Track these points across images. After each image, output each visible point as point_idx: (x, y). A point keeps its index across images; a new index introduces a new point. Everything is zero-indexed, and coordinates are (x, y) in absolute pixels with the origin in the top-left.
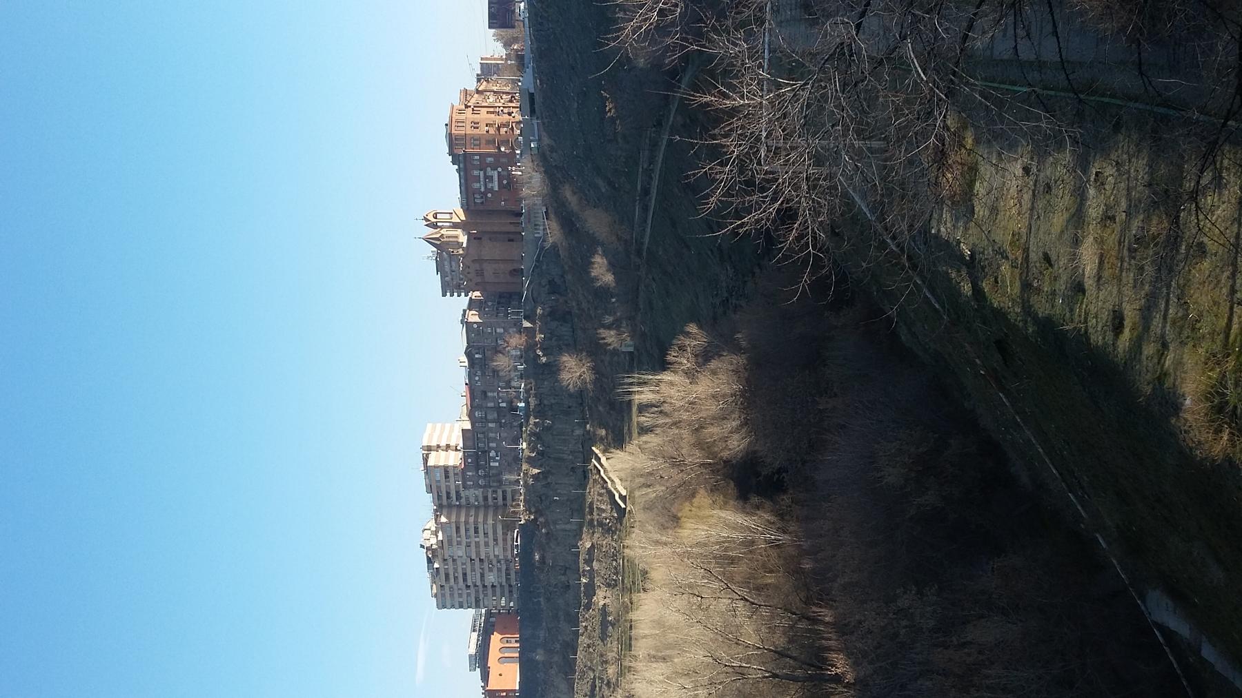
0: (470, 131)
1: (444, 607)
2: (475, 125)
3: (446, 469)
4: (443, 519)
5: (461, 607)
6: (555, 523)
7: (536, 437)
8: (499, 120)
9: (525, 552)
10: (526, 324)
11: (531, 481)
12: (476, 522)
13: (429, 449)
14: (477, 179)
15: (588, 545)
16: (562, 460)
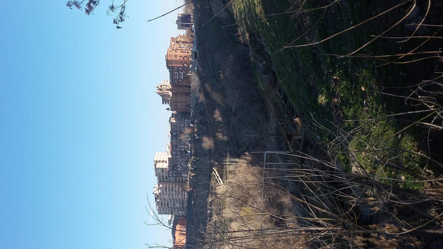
0: (174, 58)
1: (160, 214)
2: (176, 56)
3: (162, 169)
4: (161, 186)
5: (166, 214)
6: (199, 192)
7: (194, 163)
8: (184, 55)
9: (187, 197)
10: (192, 125)
11: (191, 178)
12: (172, 187)
13: (157, 162)
14: (176, 75)
15: (211, 200)
16: (203, 171)
